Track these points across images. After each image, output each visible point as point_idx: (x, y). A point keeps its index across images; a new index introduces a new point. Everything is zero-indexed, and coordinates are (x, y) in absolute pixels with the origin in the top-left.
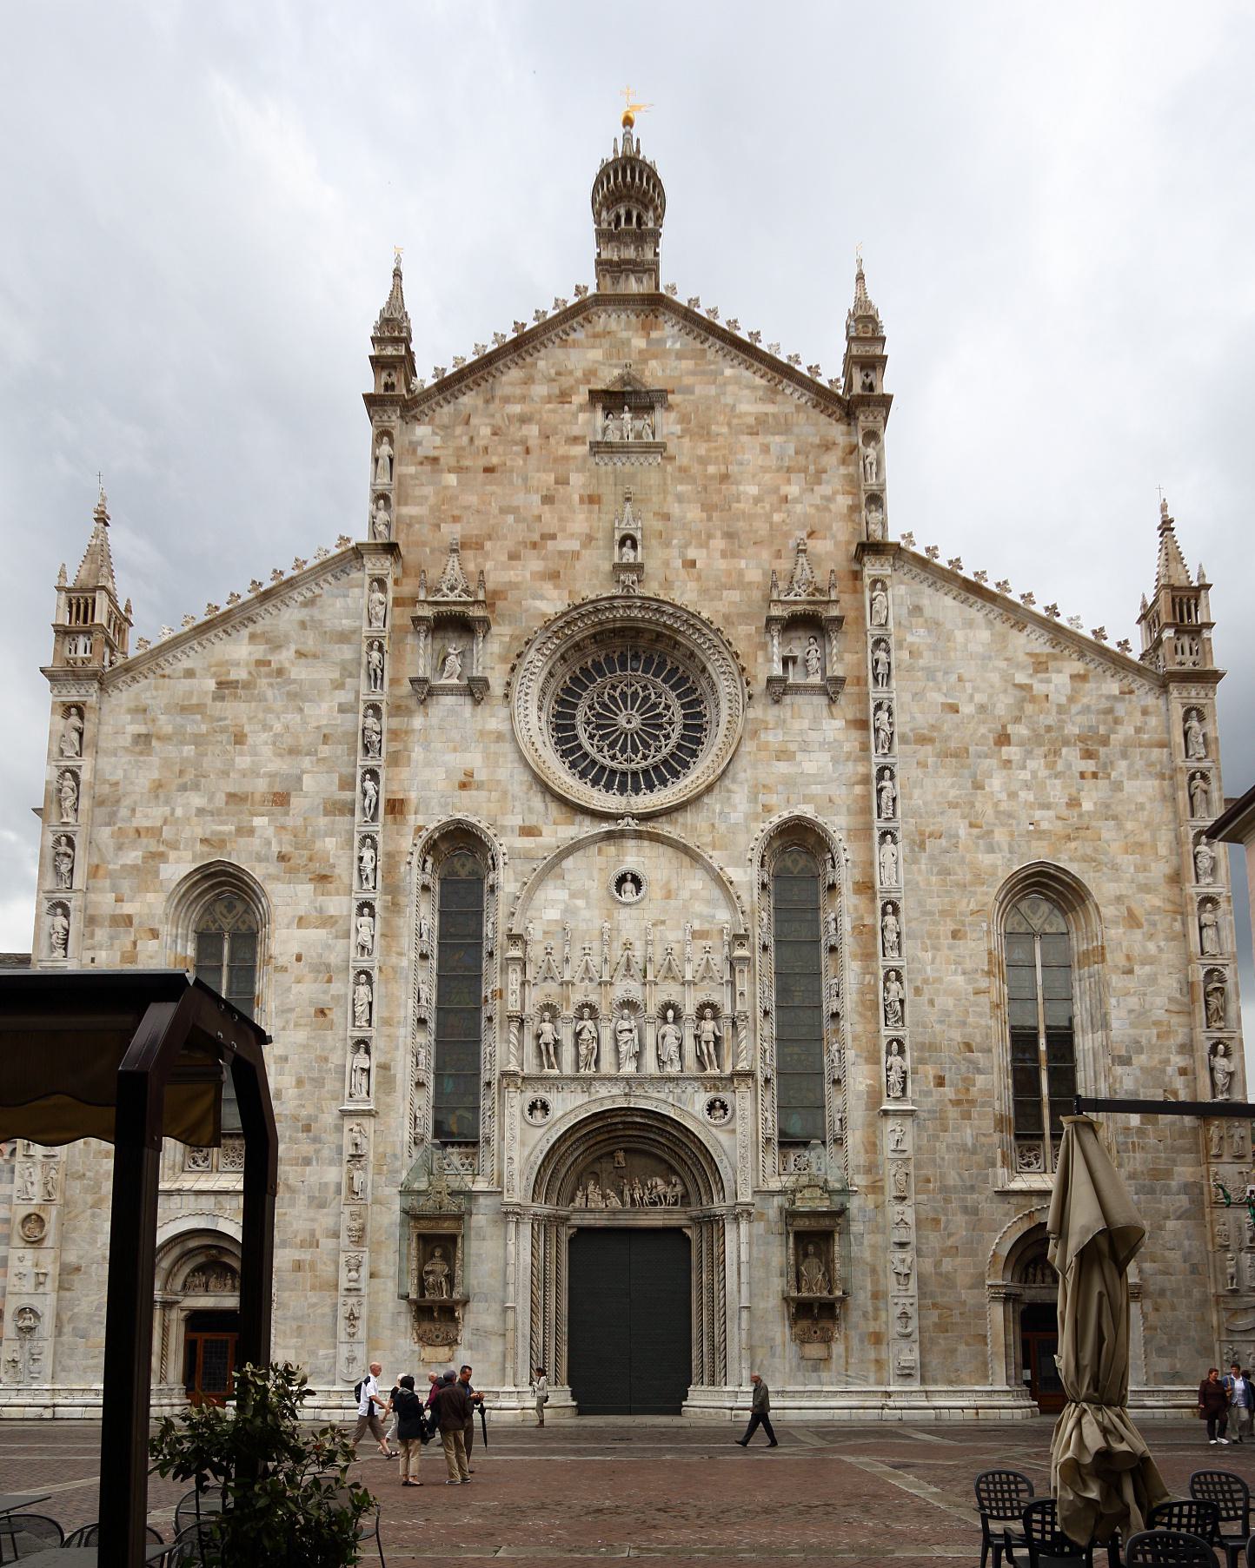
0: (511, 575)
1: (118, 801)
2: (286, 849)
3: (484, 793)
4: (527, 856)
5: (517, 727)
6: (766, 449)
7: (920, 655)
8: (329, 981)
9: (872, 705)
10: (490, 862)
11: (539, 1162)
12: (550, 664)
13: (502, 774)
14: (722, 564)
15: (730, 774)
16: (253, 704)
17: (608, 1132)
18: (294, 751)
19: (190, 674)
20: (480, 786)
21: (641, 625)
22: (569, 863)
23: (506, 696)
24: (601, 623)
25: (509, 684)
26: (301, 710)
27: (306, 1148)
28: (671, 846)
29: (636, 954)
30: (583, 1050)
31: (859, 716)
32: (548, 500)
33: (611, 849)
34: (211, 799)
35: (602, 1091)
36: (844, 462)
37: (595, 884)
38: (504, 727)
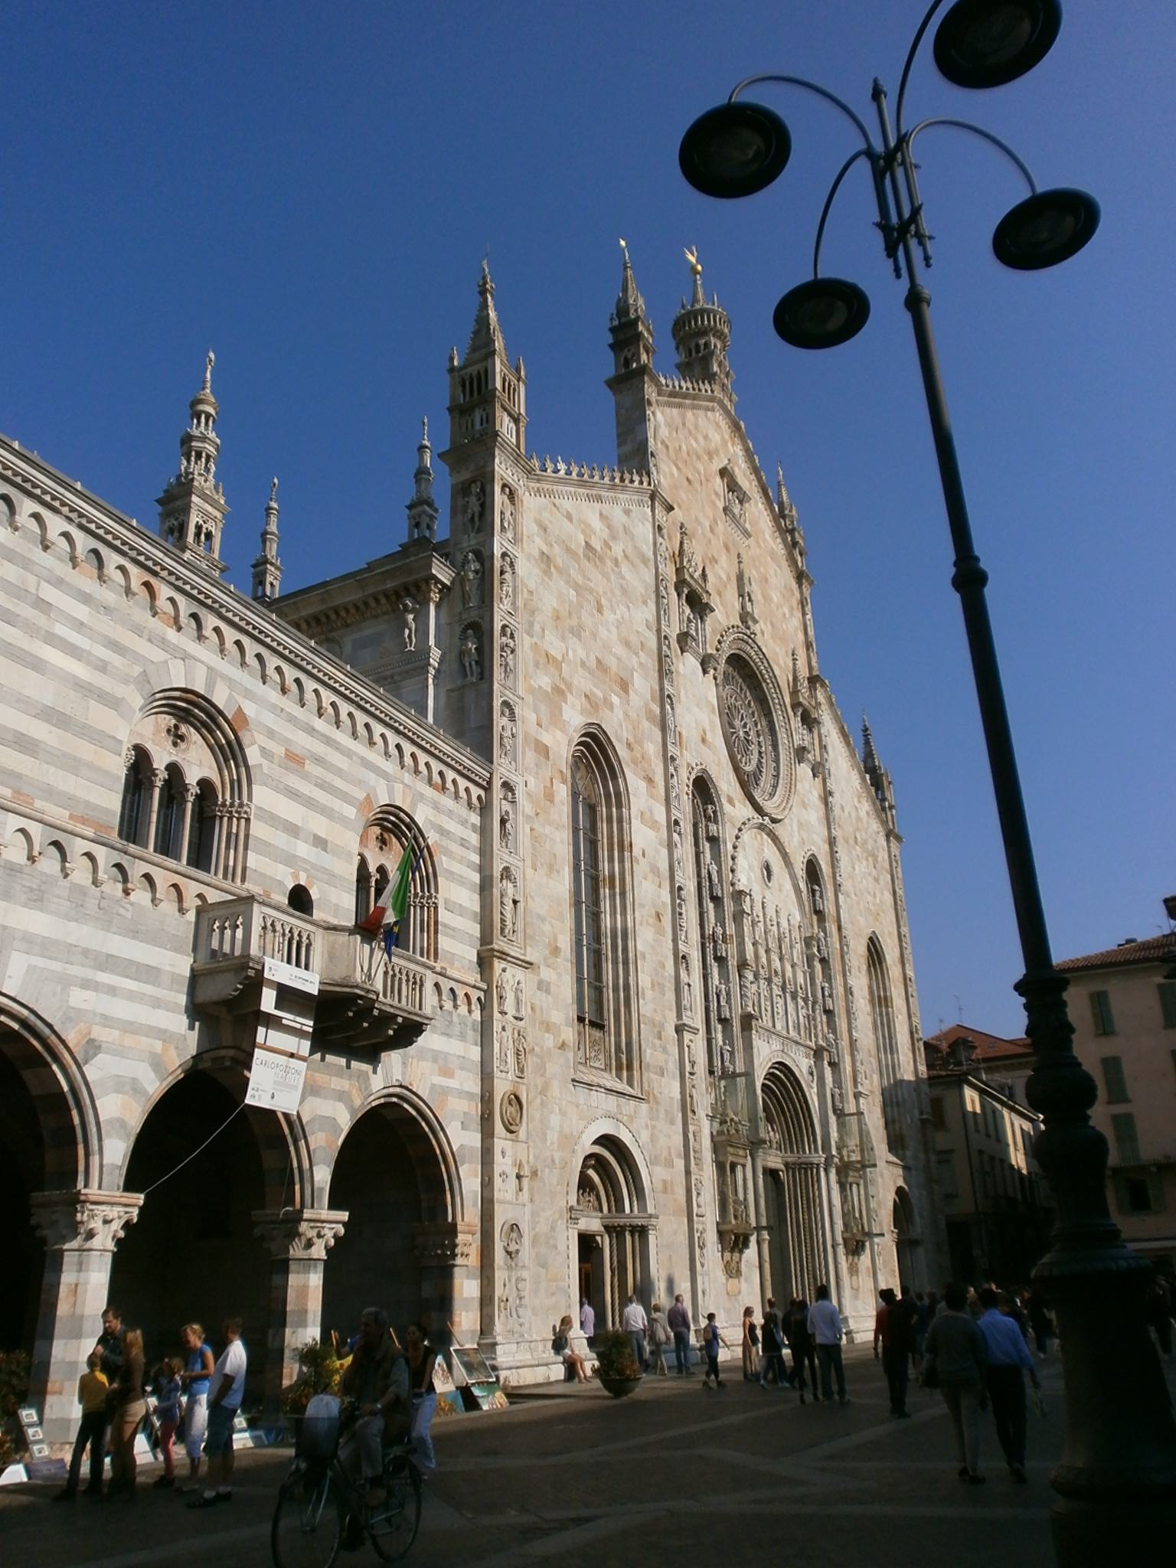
1: (533, 612)
2: (631, 739)
8: (660, 886)
14: (771, 642)
16: (605, 580)
18: (627, 644)
19: (569, 517)
26: (628, 607)
27: (660, 1057)
28: (778, 849)
34: (588, 655)
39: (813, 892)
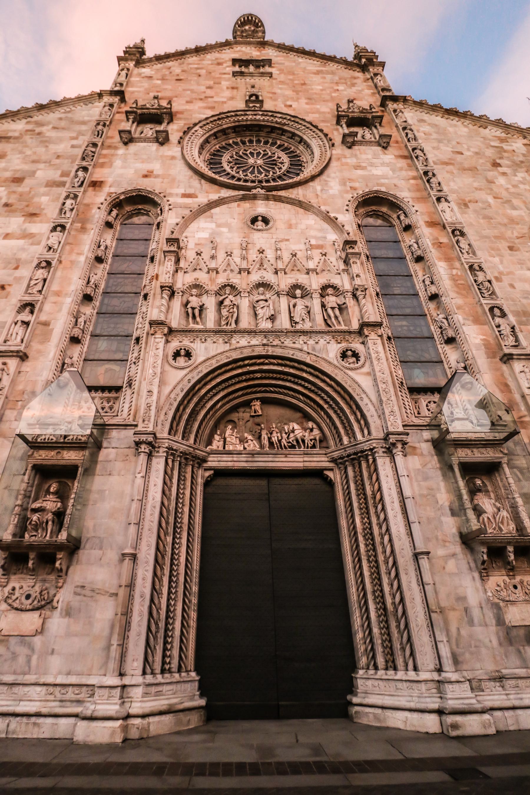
0: (188, 107)
3: (159, 180)
4: (186, 207)
5: (185, 152)
6: (325, 78)
7: (431, 135)
9: (410, 149)
10: (159, 212)
11: (179, 399)
12: (207, 135)
13: (172, 172)
15: (326, 173)
17: (246, 380)
20: (157, 176)
21: (263, 123)
22: (216, 211)
23: (179, 142)
24: (239, 121)
25: (181, 138)
29: (268, 256)
30: (224, 312)
31: (401, 154)
32: (210, 87)
33: (246, 205)
35: (243, 341)
36: (365, 82)
37: (236, 221)
38: (179, 154)
39: (398, 217)
